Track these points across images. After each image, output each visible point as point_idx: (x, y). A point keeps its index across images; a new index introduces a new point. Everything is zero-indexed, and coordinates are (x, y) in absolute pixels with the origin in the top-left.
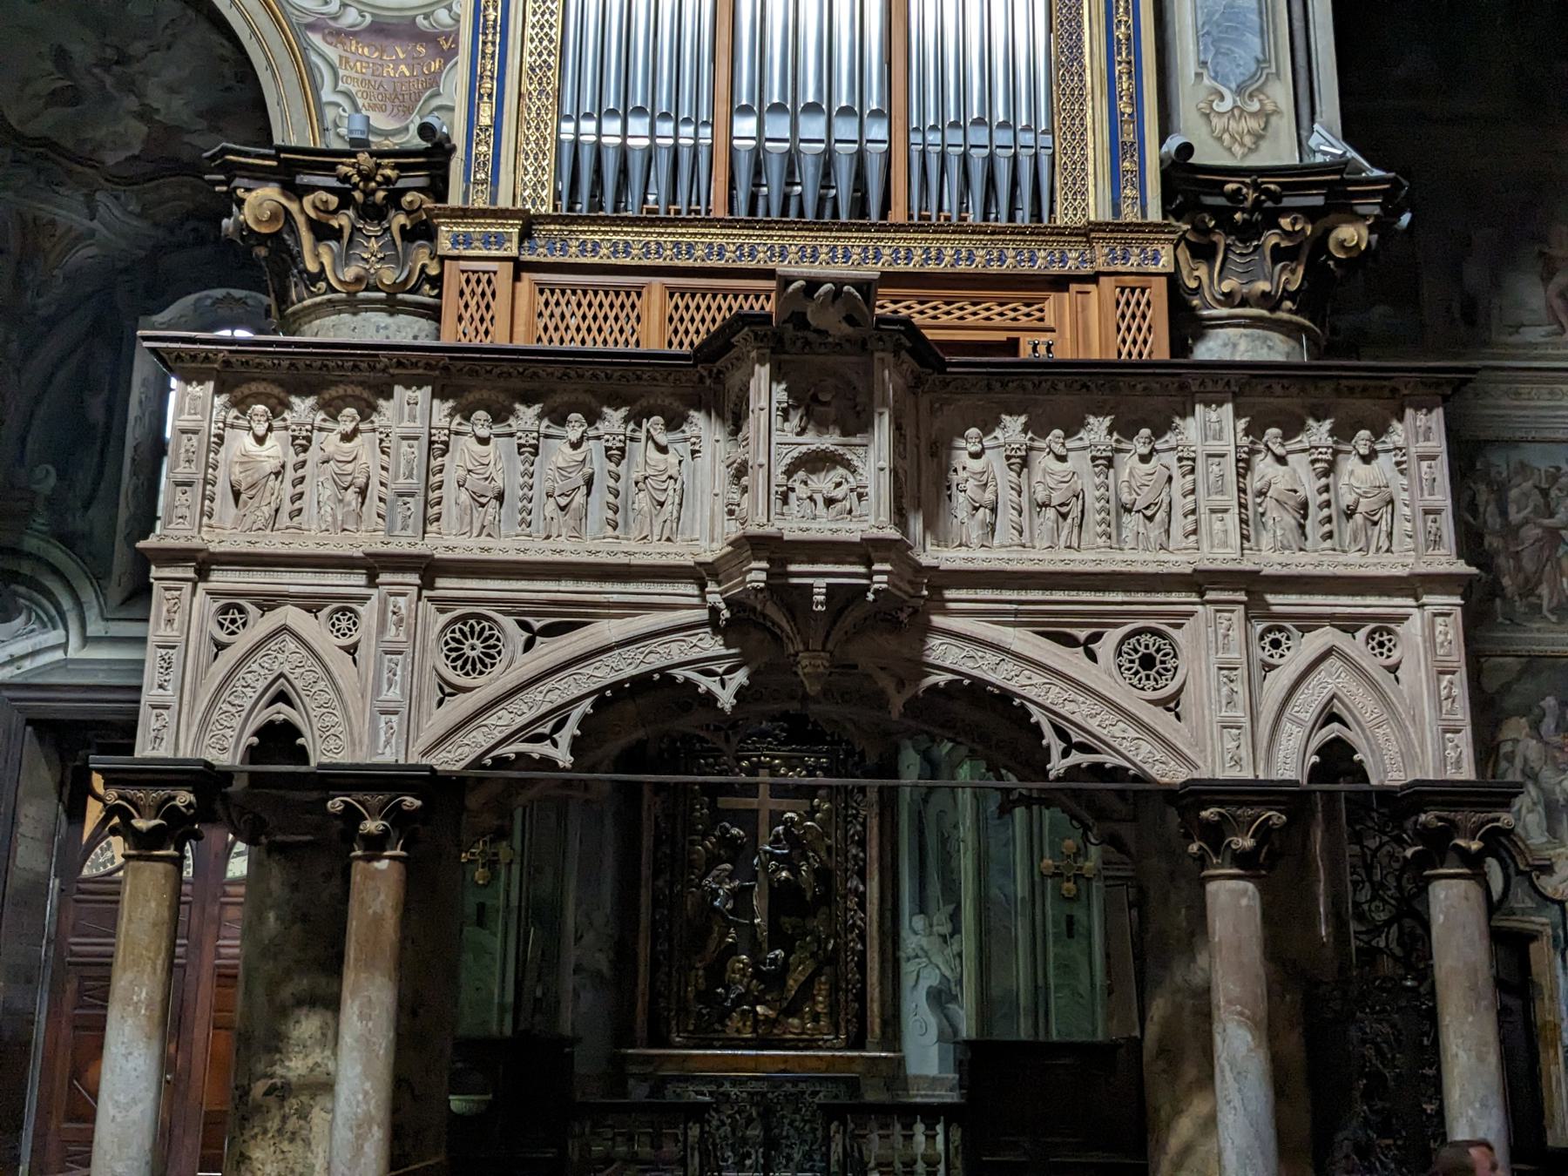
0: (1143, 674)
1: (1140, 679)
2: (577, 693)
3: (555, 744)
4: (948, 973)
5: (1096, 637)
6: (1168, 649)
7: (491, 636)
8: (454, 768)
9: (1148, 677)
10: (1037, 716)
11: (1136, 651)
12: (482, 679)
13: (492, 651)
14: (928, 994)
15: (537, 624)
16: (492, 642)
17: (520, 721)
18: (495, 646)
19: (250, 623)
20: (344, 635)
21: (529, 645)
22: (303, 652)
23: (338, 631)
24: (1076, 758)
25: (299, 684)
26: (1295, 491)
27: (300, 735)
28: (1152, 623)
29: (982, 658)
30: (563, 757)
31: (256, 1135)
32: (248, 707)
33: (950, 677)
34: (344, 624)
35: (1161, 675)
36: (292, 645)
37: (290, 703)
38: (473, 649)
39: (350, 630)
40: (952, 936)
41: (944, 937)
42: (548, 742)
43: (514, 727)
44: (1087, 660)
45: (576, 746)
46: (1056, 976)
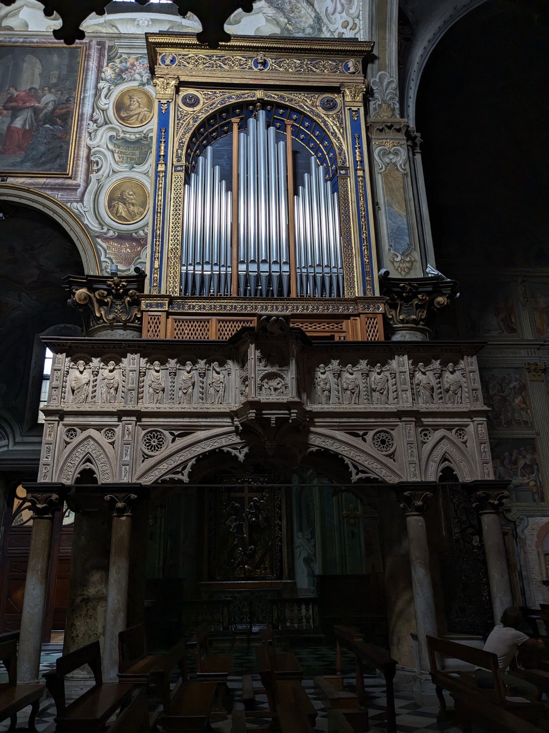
0: (382, 446)
1: (381, 448)
2: (190, 457)
3: (183, 475)
5: (365, 434)
6: (390, 437)
7: (161, 438)
8: (148, 484)
9: (383, 447)
10: (347, 461)
11: (379, 438)
12: (157, 453)
13: (161, 443)
15: (176, 433)
16: (161, 440)
17: (171, 467)
18: (162, 441)
19: (78, 435)
20: (110, 438)
21: (173, 441)
22: (96, 445)
23: (108, 437)
24: (361, 475)
25: (94, 456)
26: (429, 384)
27: (95, 473)
28: (384, 429)
29: (328, 441)
30: (185, 479)
32: (77, 464)
33: (317, 448)
34: (110, 435)
35: (388, 446)
36: (92, 442)
37: (91, 463)
38: (154, 442)
39: (112, 437)
42: (180, 474)
43: (169, 469)
44: (363, 442)
45: (190, 475)
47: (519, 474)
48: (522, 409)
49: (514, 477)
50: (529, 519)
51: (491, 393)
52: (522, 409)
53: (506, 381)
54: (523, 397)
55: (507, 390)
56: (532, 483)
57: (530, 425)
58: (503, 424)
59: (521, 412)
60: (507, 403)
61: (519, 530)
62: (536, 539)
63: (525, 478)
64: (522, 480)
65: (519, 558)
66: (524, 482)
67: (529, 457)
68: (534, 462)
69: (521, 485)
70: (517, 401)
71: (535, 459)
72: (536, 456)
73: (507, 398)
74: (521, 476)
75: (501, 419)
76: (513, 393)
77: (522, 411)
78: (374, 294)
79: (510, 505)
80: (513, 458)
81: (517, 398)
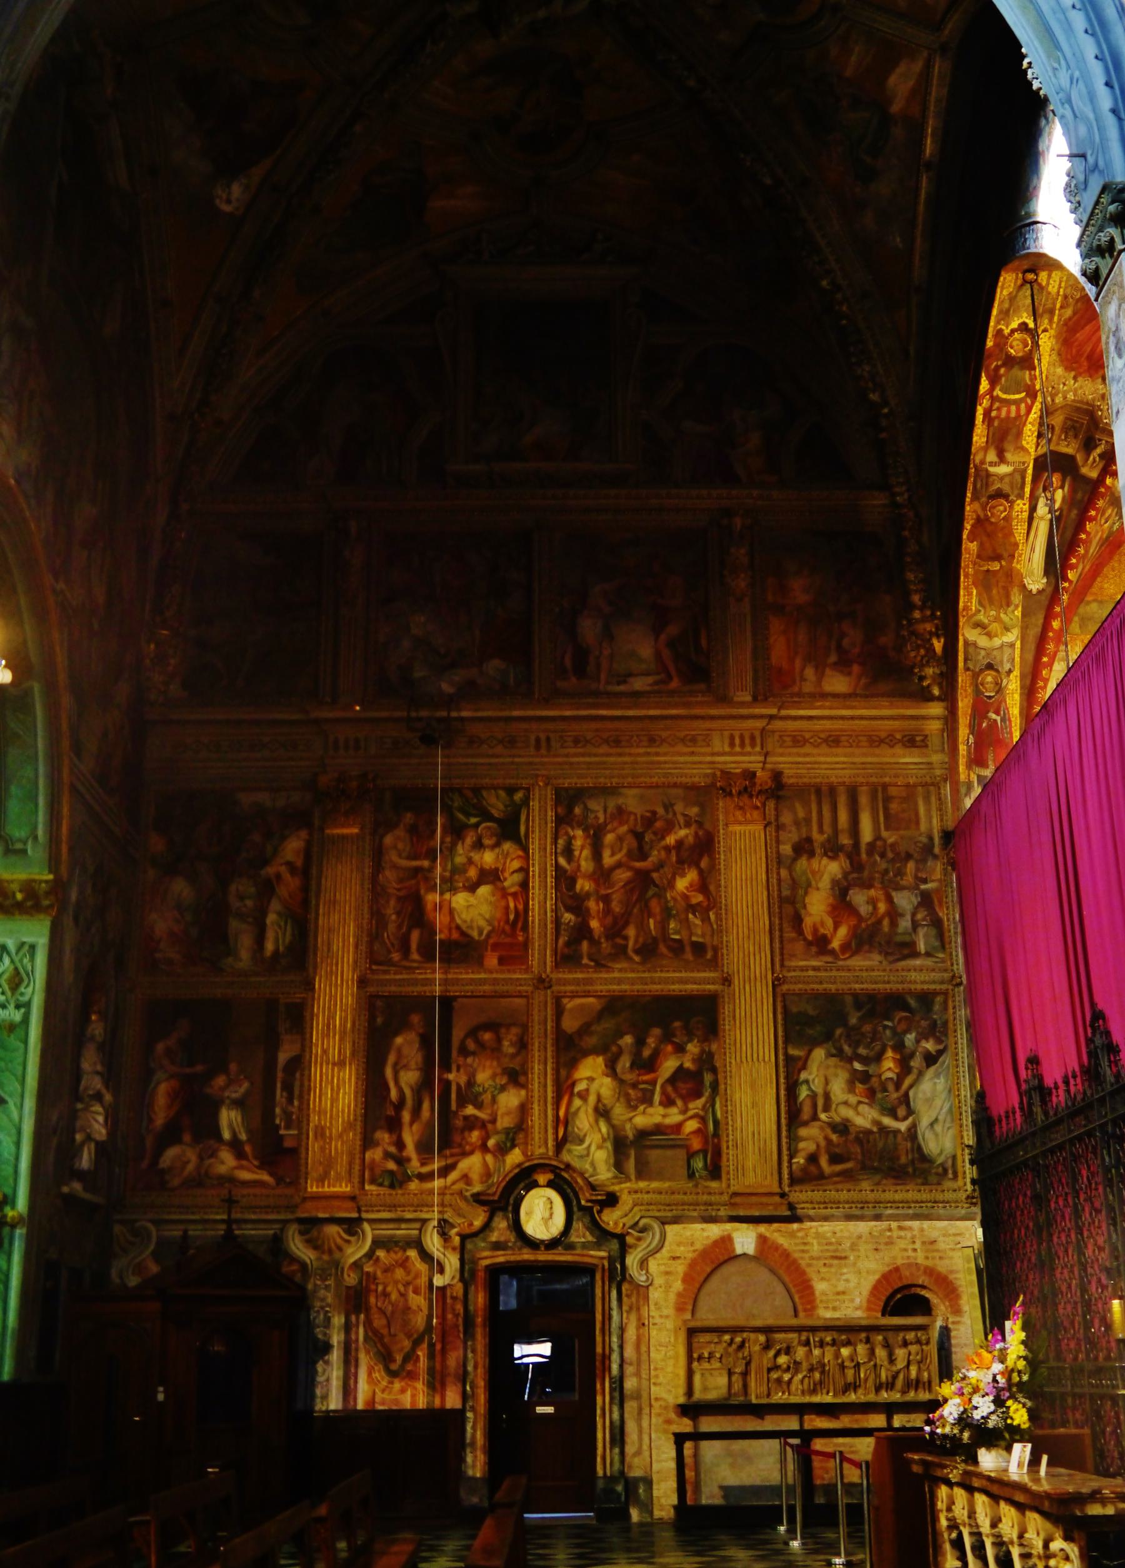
47: (657, 1098)
48: (693, 908)
49: (642, 1108)
50: (669, 1228)
51: (608, 860)
52: (693, 908)
53: (658, 824)
54: (701, 872)
55: (655, 853)
56: (692, 1126)
57: (709, 955)
59: (691, 916)
60: (650, 893)
61: (632, 1260)
63: (674, 1110)
64: (664, 1116)
66: (668, 1121)
67: (693, 1048)
68: (707, 1062)
69: (659, 1129)
70: (682, 884)
71: (711, 1055)
72: (714, 1047)
73: (655, 875)
74: (661, 1103)
75: (626, 938)
76: (674, 859)
77: (694, 914)
79: (616, 1188)
80: (646, 1053)
81: (683, 875)
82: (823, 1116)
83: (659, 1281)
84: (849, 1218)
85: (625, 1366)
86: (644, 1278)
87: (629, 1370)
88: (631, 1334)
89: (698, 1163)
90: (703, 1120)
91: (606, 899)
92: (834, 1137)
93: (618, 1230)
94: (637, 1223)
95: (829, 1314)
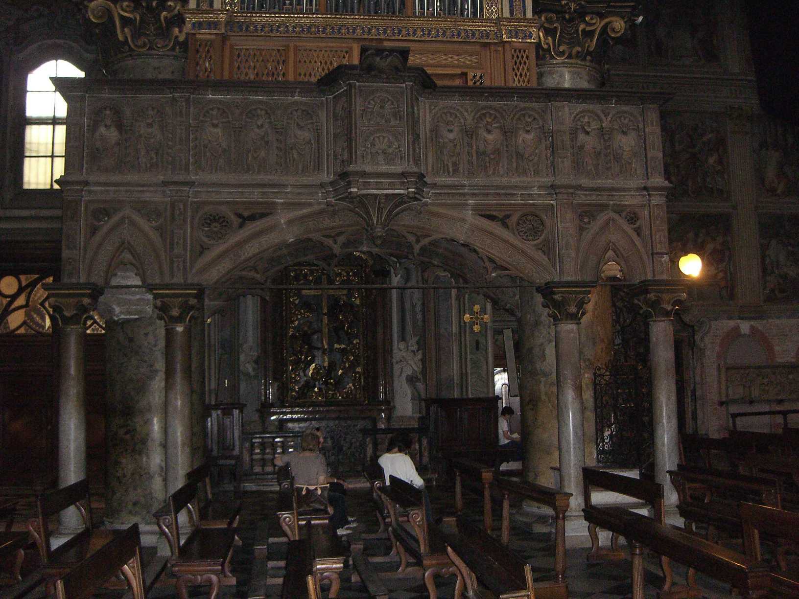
4: (416, 369)
14: (407, 379)
31: (122, 452)
38: (215, 227)
40: (417, 351)
41: (413, 351)
46: (472, 368)
50: (712, 322)
51: (678, 147)
58: (690, 193)
61: (697, 337)
62: (717, 349)
65: (694, 372)
70: (711, 160)
78: (525, 14)
80: (700, 240)
82: (776, 271)
83: (709, 346)
84: (789, 317)
85: (697, 386)
86: (703, 345)
87: (698, 386)
88: (698, 371)
89: (724, 293)
90: (726, 273)
91: (678, 167)
92: (781, 281)
93: (691, 324)
94: (699, 321)
95: (781, 360)
